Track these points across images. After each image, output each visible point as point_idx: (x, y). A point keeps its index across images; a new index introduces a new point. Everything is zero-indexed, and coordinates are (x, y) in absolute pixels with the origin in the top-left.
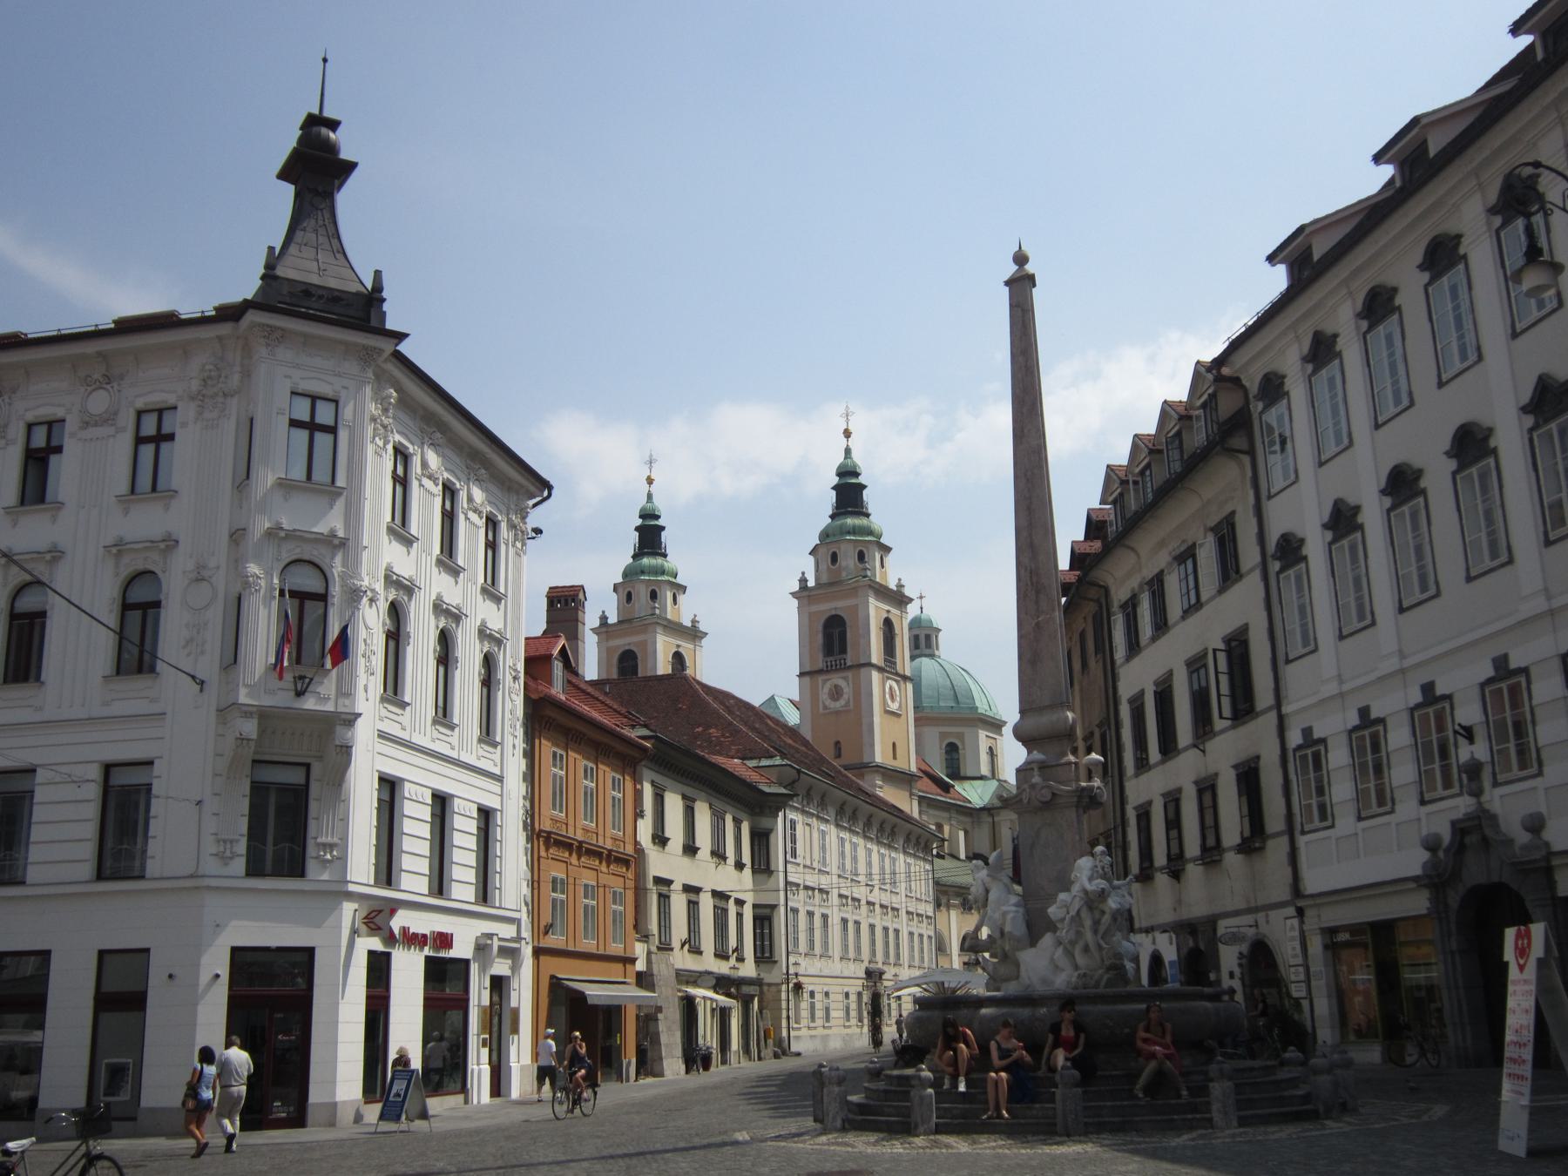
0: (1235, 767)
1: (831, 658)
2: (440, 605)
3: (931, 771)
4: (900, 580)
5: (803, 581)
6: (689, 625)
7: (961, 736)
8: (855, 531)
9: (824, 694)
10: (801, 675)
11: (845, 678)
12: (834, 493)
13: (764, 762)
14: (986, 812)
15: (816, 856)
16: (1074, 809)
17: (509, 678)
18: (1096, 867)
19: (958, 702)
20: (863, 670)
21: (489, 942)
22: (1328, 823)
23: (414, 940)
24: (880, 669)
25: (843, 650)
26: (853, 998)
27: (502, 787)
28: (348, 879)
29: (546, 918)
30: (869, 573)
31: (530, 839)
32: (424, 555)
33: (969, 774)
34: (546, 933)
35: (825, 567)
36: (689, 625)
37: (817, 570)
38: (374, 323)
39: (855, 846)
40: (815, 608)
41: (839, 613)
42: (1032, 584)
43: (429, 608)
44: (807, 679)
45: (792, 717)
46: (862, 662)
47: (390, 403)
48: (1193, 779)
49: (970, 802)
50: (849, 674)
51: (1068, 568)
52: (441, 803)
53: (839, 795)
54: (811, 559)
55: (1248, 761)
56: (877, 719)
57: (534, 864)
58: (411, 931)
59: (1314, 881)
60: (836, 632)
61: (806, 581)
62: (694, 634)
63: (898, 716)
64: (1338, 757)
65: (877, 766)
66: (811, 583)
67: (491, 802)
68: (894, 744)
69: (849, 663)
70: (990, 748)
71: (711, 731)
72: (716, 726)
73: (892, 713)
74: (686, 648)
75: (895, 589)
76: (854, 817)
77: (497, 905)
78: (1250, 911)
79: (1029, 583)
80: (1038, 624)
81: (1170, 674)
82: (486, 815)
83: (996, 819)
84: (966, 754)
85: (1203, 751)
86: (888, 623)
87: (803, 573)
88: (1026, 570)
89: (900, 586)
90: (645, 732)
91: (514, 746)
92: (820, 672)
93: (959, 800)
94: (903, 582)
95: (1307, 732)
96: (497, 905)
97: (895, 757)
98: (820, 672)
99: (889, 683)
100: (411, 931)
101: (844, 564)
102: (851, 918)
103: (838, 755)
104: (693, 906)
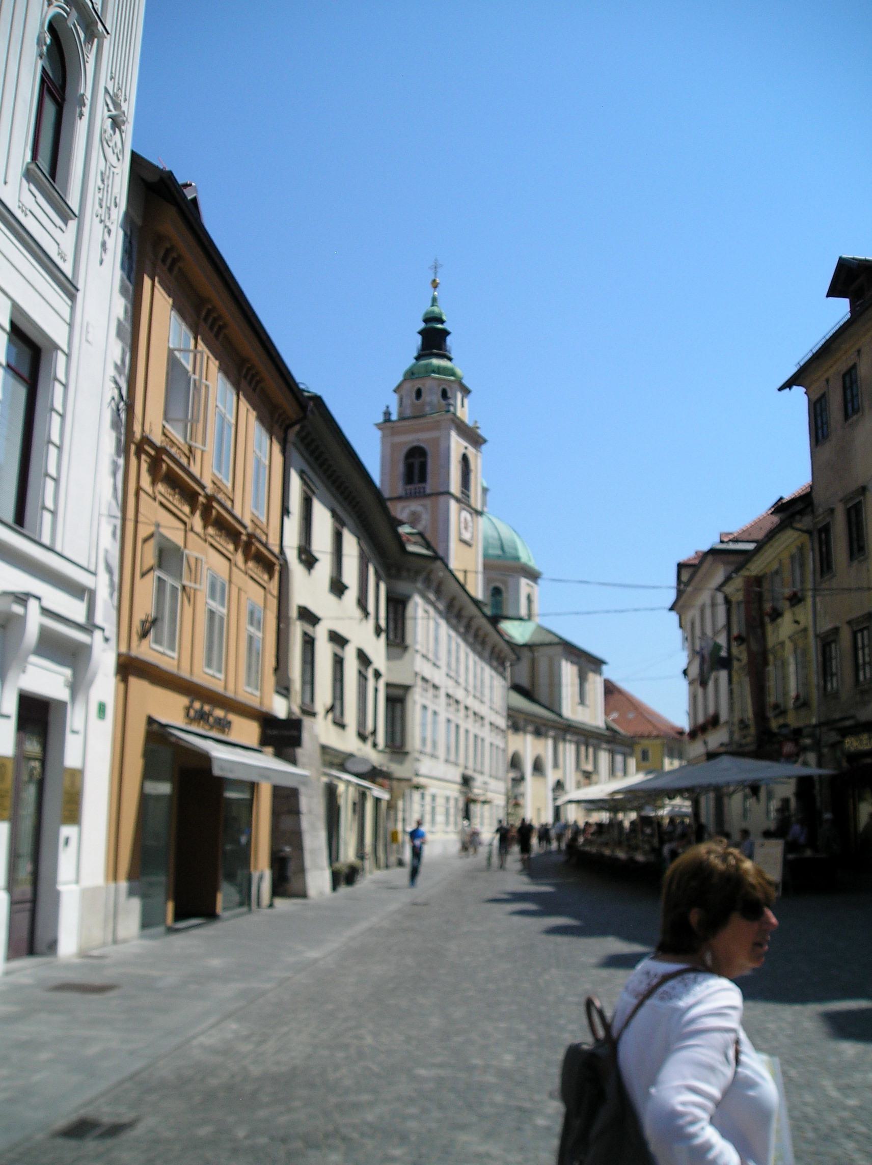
1: (409, 487)
5: (387, 414)
8: (440, 370)
12: (419, 339)
20: (442, 499)
21: (17, 609)
24: (458, 500)
25: (423, 479)
26: (452, 803)
29: (145, 607)
30: (452, 409)
34: (144, 635)
50: (428, 502)
60: (417, 462)
66: (394, 417)
69: (428, 491)
83: (536, 654)
86: (465, 459)
87: (388, 407)
91: (104, 245)
96: (46, 540)
98: (399, 498)
99: (465, 514)
104: (339, 662)
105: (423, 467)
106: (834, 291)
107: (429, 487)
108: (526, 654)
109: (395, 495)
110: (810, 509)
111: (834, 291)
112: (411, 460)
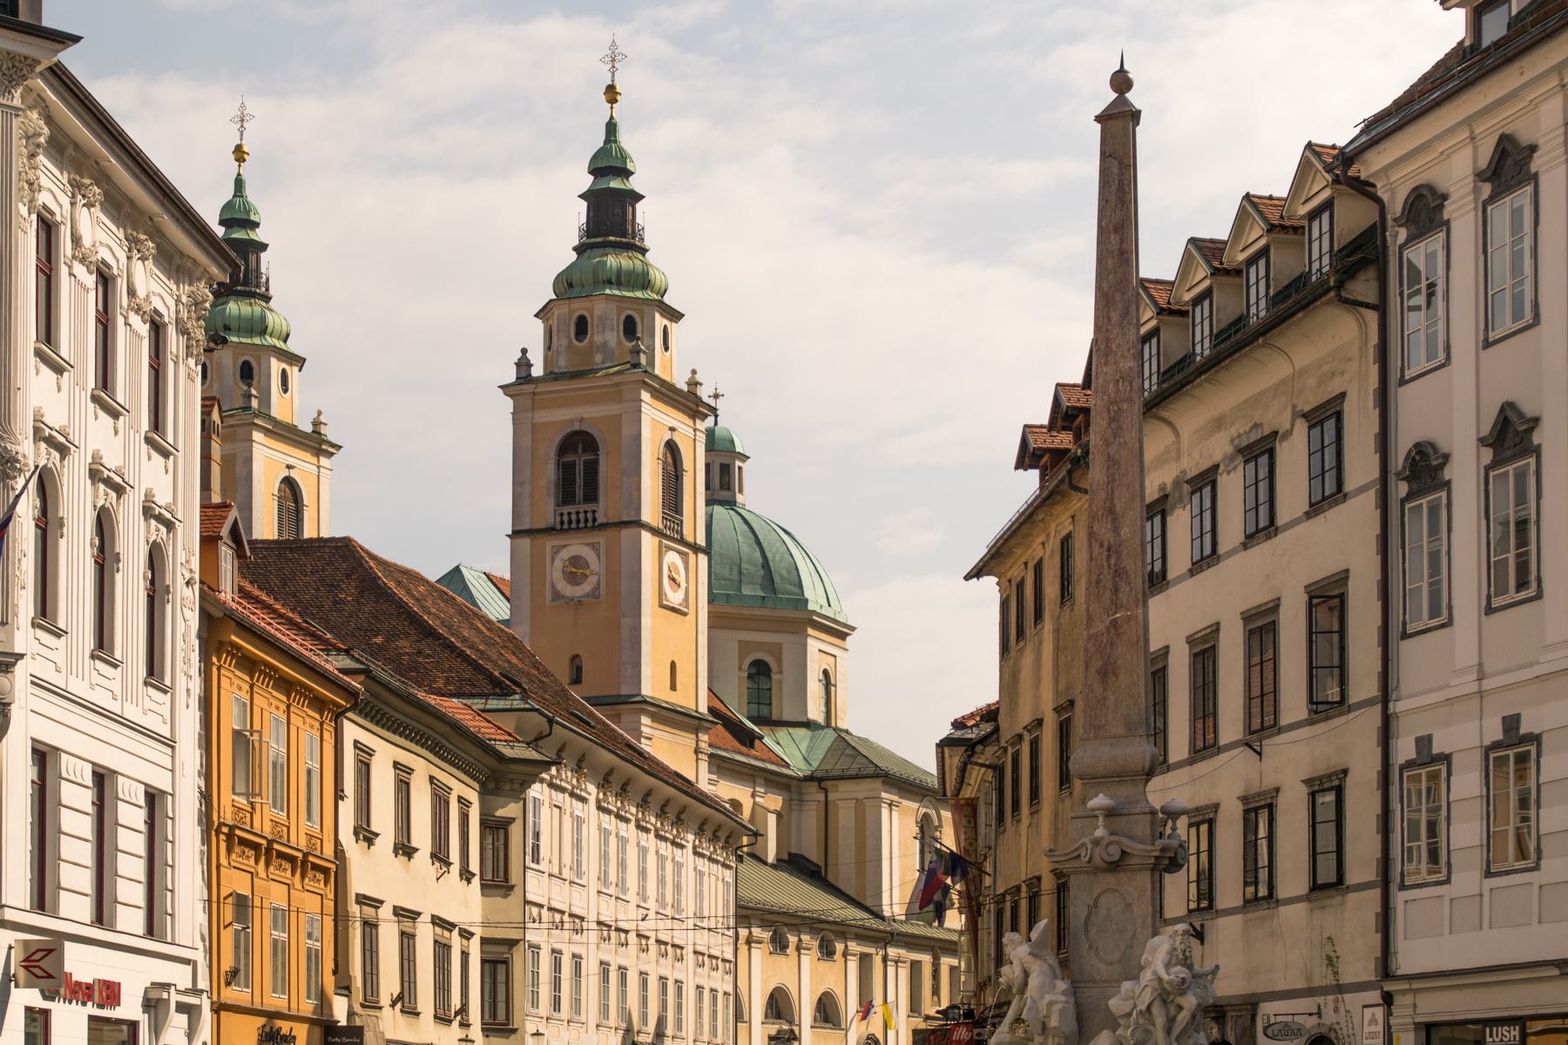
0: (1306, 782)
1: (565, 510)
2: (98, 471)
3: (723, 709)
4: (694, 372)
5: (523, 364)
6: (309, 429)
7: (777, 650)
9: (555, 572)
10: (516, 534)
11: (592, 545)
13: (494, 704)
14: (816, 783)
15: (567, 860)
16: (1149, 873)
17: (180, 582)
18: (1175, 949)
19: (774, 591)
20: (626, 533)
22: (1442, 877)
23: (81, 992)
24: (655, 531)
25: (592, 495)
27: (173, 757)
28: (4, 902)
29: (227, 963)
30: (643, 359)
31: (206, 839)
32: (77, 388)
33: (786, 717)
35: (564, 342)
36: (309, 429)
37: (548, 347)
38: (24, 16)
39: (623, 842)
40: (543, 416)
41: (584, 428)
42: (1109, 567)
43: (84, 472)
44: (526, 542)
45: (495, 607)
46: (625, 519)
47: (38, 146)
48: (1240, 794)
49: (787, 766)
50: (600, 538)
51: (1045, 421)
52: (102, 779)
53: (607, 758)
54: (539, 325)
55: (1329, 776)
56: (646, 621)
57: (212, 877)
58: (74, 979)
59: (1412, 956)
61: (530, 365)
62: (316, 443)
63: (685, 614)
64: (1466, 783)
65: (645, 702)
66: (537, 371)
67: (162, 781)
68: (673, 665)
69: (601, 519)
70: (825, 672)
71: (400, 643)
72: (407, 635)
73: (673, 610)
74: (304, 466)
75: (685, 388)
76: (623, 791)
77: (169, 940)
78: (1309, 992)
79: (1105, 564)
80: (1114, 623)
81: (1216, 628)
82: (154, 799)
83: (832, 796)
84: (782, 681)
85: (1260, 754)
86: (671, 447)
87: (524, 351)
88: (1101, 545)
89: (694, 384)
90: (347, 663)
91: (188, 690)
92: (549, 530)
93: (772, 763)
94: (698, 378)
95: (1424, 742)
96: (169, 940)
97: (673, 687)
98: (549, 530)
100: (74, 979)
101: (598, 339)
102: (614, 962)
103: (577, 680)
105: (592, 469)
106: (1022, 464)
107: (606, 508)
108: (814, 794)
109: (543, 526)
110: (995, 736)
111: (1022, 464)
112: (569, 458)
